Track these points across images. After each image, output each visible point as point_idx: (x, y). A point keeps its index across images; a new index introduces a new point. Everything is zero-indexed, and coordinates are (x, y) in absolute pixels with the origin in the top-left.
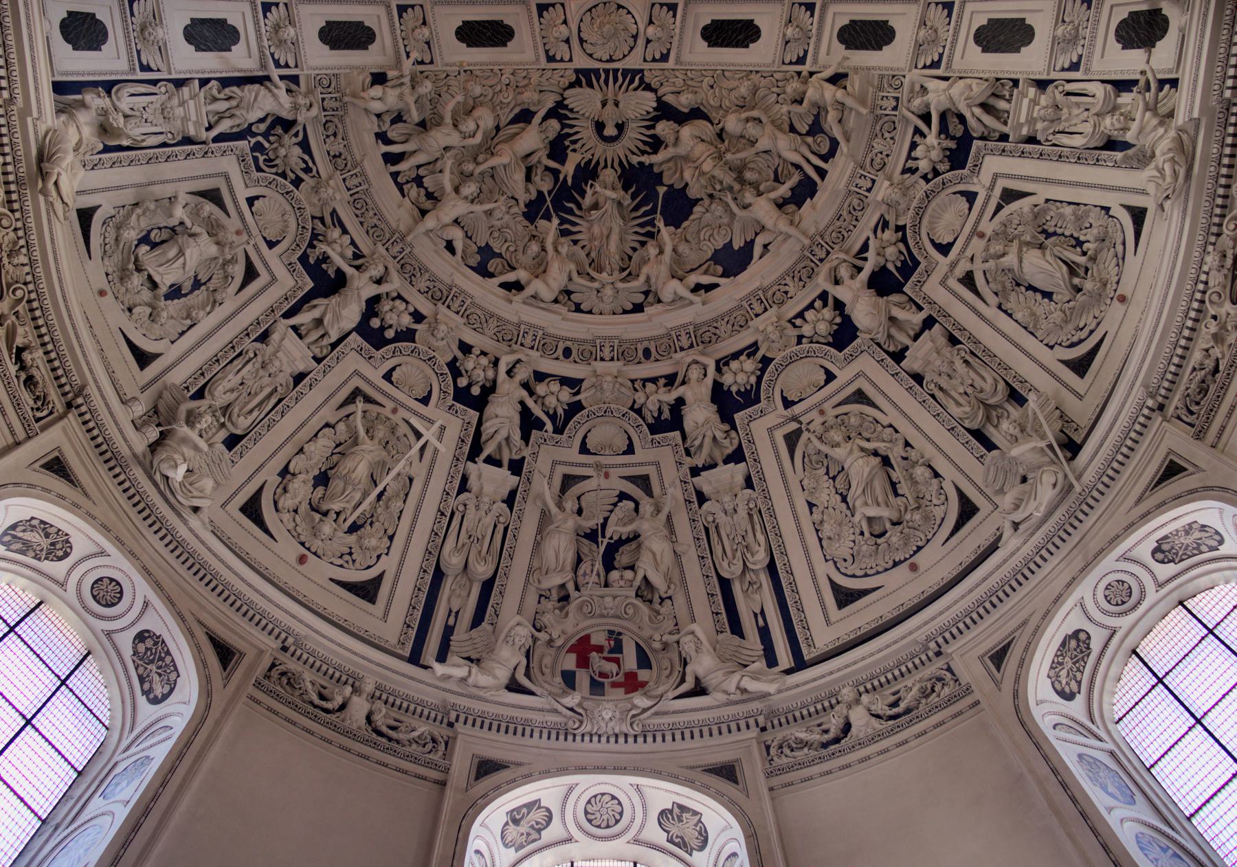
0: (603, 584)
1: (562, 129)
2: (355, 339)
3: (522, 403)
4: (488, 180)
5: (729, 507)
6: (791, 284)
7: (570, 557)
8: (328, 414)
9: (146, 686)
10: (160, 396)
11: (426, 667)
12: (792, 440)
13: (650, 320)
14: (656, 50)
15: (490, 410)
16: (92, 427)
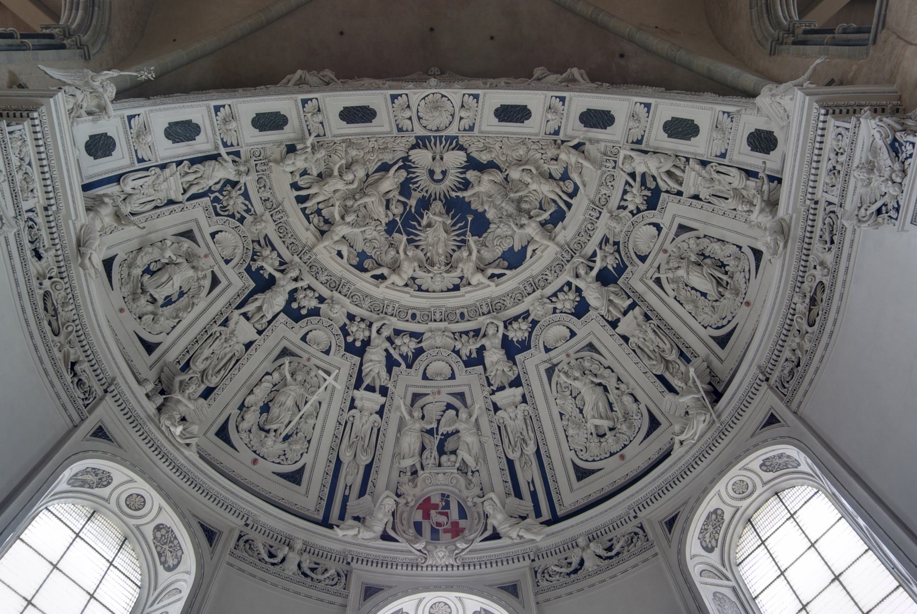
0: (437, 463)
1: (408, 175)
2: (283, 317)
3: (386, 350)
4: (363, 210)
5: (513, 416)
6: (550, 275)
7: (418, 446)
8: (267, 366)
9: (163, 559)
10: (162, 371)
11: (331, 527)
12: (550, 372)
13: (463, 296)
14: (466, 123)
15: (367, 356)
16: (121, 403)
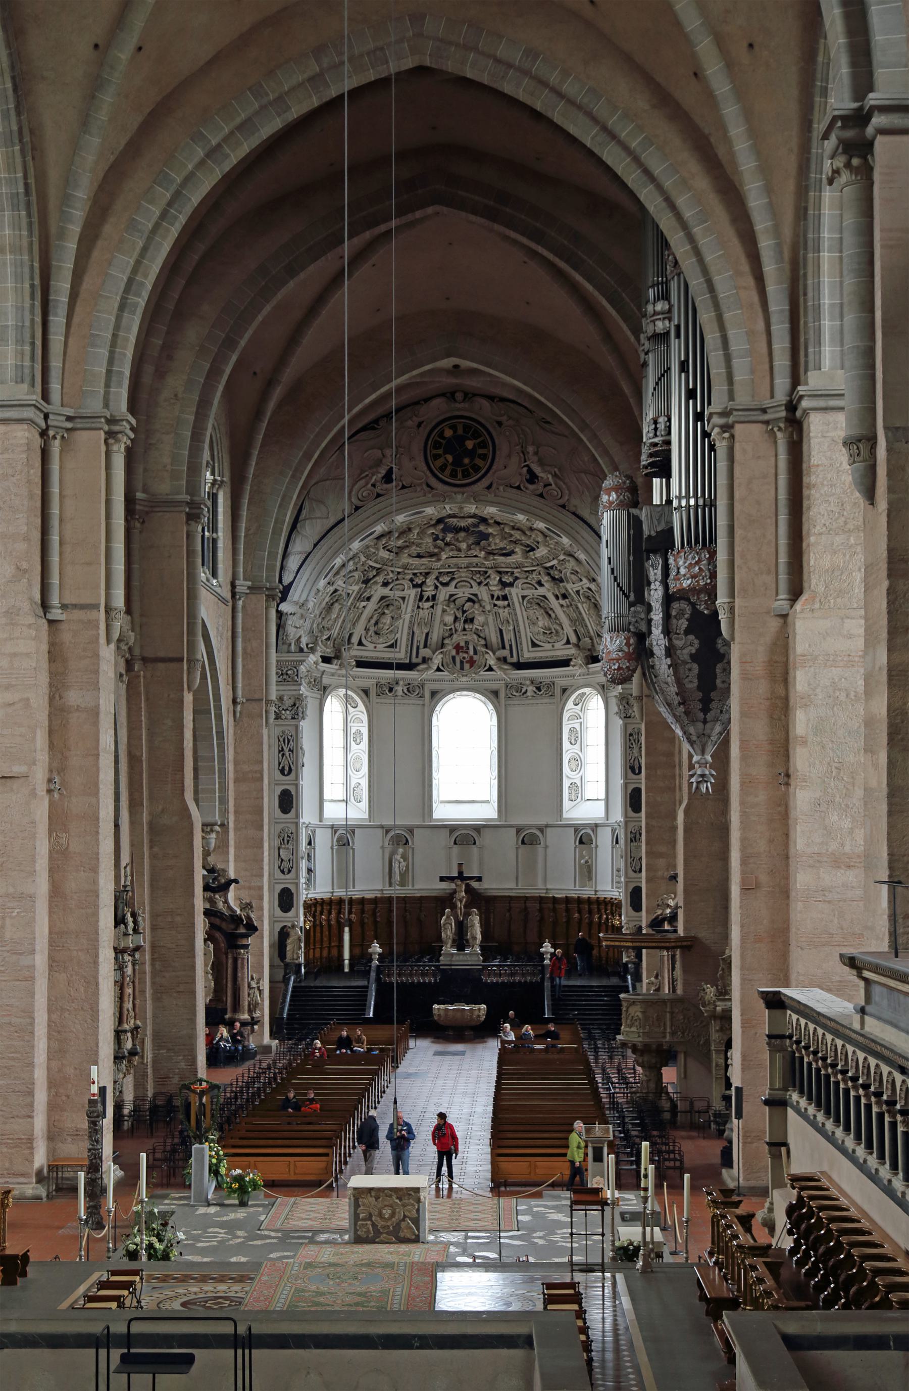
12: (524, 597)
15: (425, 588)
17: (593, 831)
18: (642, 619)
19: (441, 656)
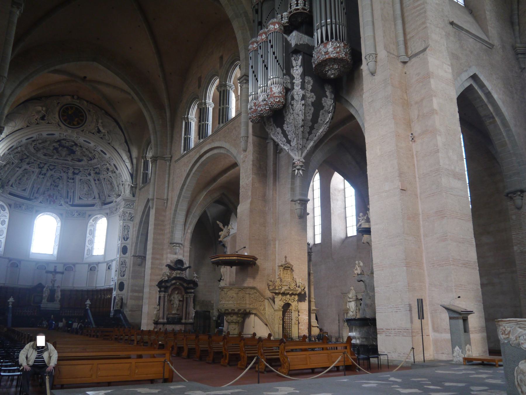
7: (50, 184)
12: (80, 180)
15: (43, 169)
17: (97, 265)
18: (289, 83)
19: (43, 197)
